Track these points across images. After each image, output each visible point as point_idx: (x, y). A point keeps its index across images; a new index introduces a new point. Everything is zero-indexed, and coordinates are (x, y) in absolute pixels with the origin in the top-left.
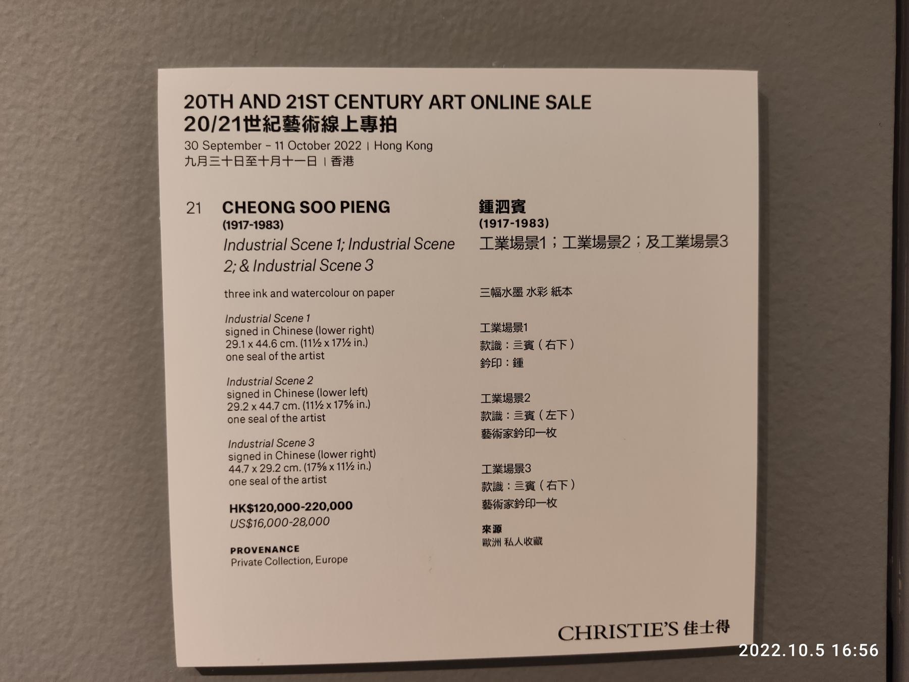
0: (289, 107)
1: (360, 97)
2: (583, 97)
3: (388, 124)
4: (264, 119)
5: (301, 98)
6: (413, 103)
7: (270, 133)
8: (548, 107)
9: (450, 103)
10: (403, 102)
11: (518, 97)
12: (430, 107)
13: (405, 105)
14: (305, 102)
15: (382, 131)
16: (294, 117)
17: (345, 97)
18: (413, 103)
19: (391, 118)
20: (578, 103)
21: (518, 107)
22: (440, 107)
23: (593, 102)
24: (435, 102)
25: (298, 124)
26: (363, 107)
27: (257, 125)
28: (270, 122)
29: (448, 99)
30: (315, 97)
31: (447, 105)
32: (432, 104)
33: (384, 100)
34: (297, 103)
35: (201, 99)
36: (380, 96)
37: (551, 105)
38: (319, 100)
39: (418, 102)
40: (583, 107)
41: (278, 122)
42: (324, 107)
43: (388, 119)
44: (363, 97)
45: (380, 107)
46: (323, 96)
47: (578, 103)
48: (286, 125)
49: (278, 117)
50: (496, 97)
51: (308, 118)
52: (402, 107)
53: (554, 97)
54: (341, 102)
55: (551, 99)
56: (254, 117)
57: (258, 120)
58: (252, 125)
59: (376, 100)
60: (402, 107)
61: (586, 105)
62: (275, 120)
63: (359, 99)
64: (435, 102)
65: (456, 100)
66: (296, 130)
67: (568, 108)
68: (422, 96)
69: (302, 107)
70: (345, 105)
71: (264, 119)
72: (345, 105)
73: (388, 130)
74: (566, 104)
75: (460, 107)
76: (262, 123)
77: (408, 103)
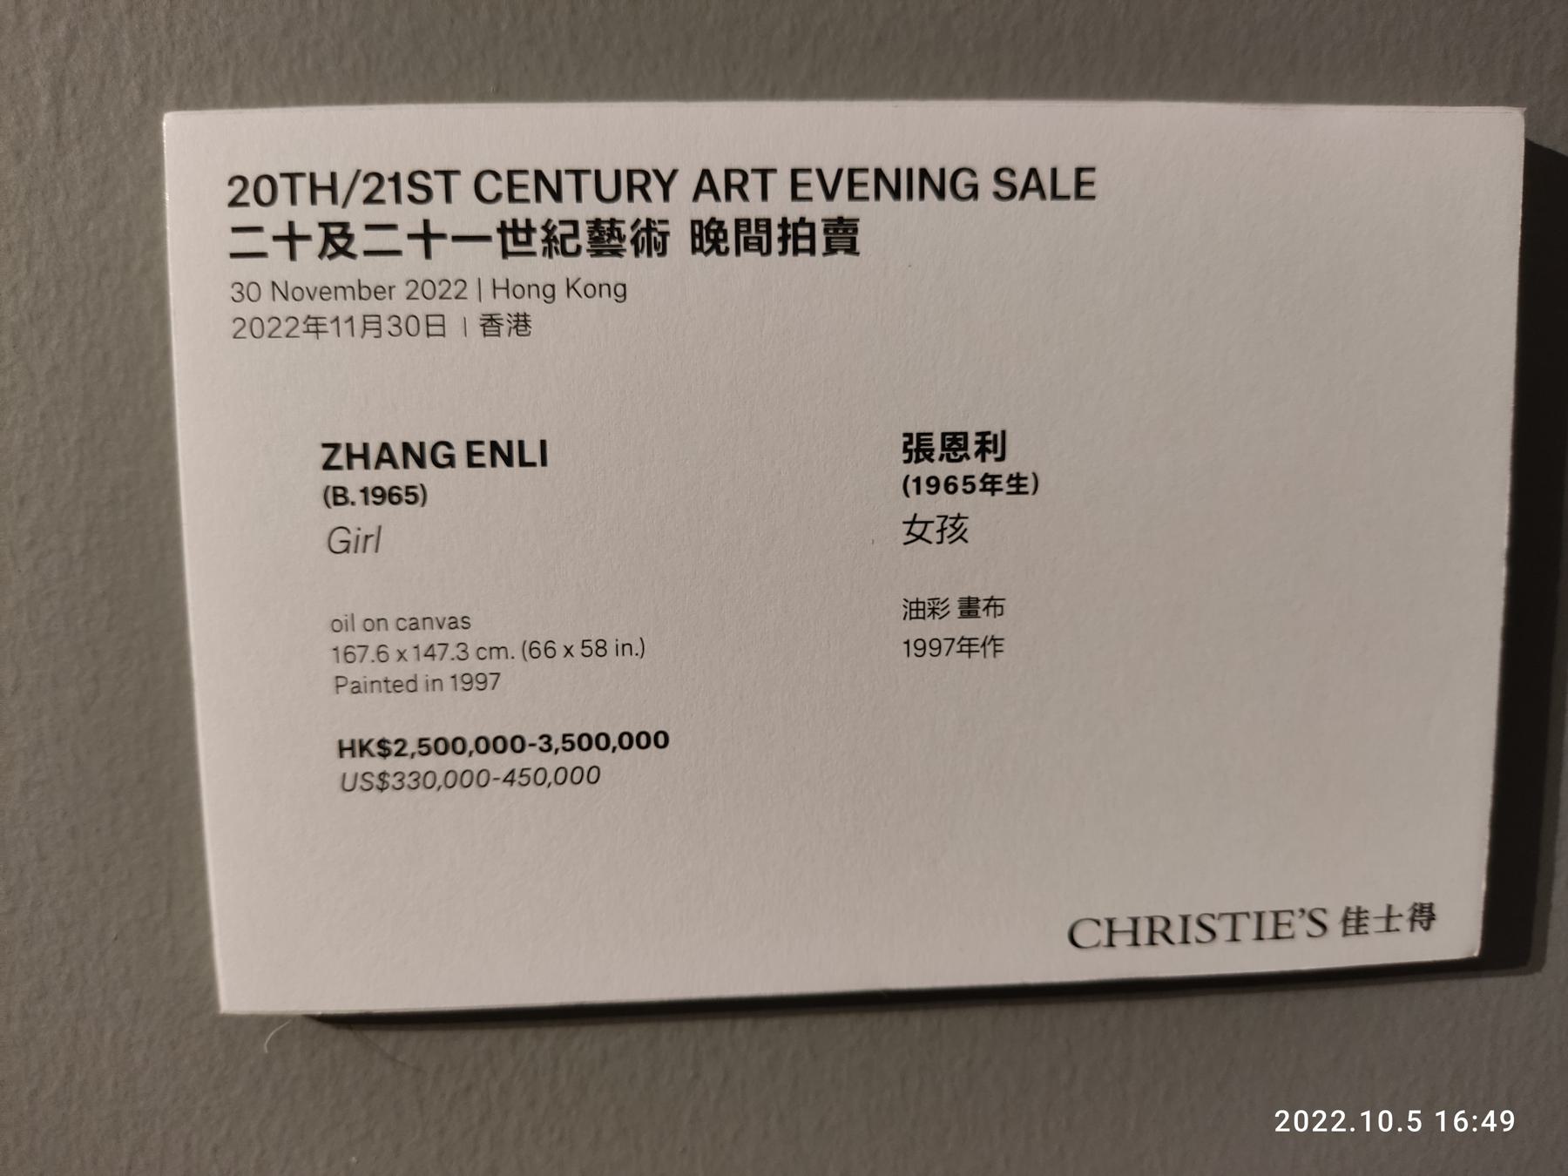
0: (369, 200)
1: (532, 175)
2: (1079, 171)
3: (797, 237)
4: (545, 228)
5: (396, 179)
6: (655, 188)
7: (558, 258)
8: (997, 194)
9: (740, 188)
10: (631, 186)
11: (924, 173)
12: (696, 198)
13: (637, 193)
14: (406, 188)
15: (783, 252)
16: (612, 221)
17: (497, 176)
18: (655, 188)
19: (802, 221)
20: (1066, 185)
21: (922, 196)
22: (717, 198)
23: (1100, 182)
24: (706, 185)
25: (622, 238)
26: (538, 199)
27: (528, 242)
28: (557, 233)
29: (736, 178)
30: (426, 175)
31: (734, 192)
32: (699, 190)
33: (588, 182)
34: (388, 191)
35: (265, 184)
36: (578, 173)
37: (1006, 191)
38: (437, 184)
39: (666, 186)
40: (1078, 195)
41: (575, 235)
42: (448, 199)
43: (796, 226)
44: (539, 175)
45: (579, 198)
46: (447, 174)
47: (1066, 185)
48: (593, 240)
49: (575, 223)
50: (898, 171)
51: (643, 224)
52: (631, 198)
53: (1013, 173)
54: (490, 187)
55: (1005, 176)
56: (522, 224)
57: (529, 229)
58: (516, 242)
59: (568, 182)
60: (631, 198)
61: (1085, 190)
62: (569, 229)
63: (529, 179)
64: (706, 185)
65: (755, 179)
66: (616, 252)
67: (1043, 196)
68: (674, 172)
69: (398, 200)
70: (499, 196)
71: (545, 228)
72: (499, 196)
73: (796, 251)
74: (1039, 187)
75: (764, 196)
76: (540, 234)
77: (642, 188)
